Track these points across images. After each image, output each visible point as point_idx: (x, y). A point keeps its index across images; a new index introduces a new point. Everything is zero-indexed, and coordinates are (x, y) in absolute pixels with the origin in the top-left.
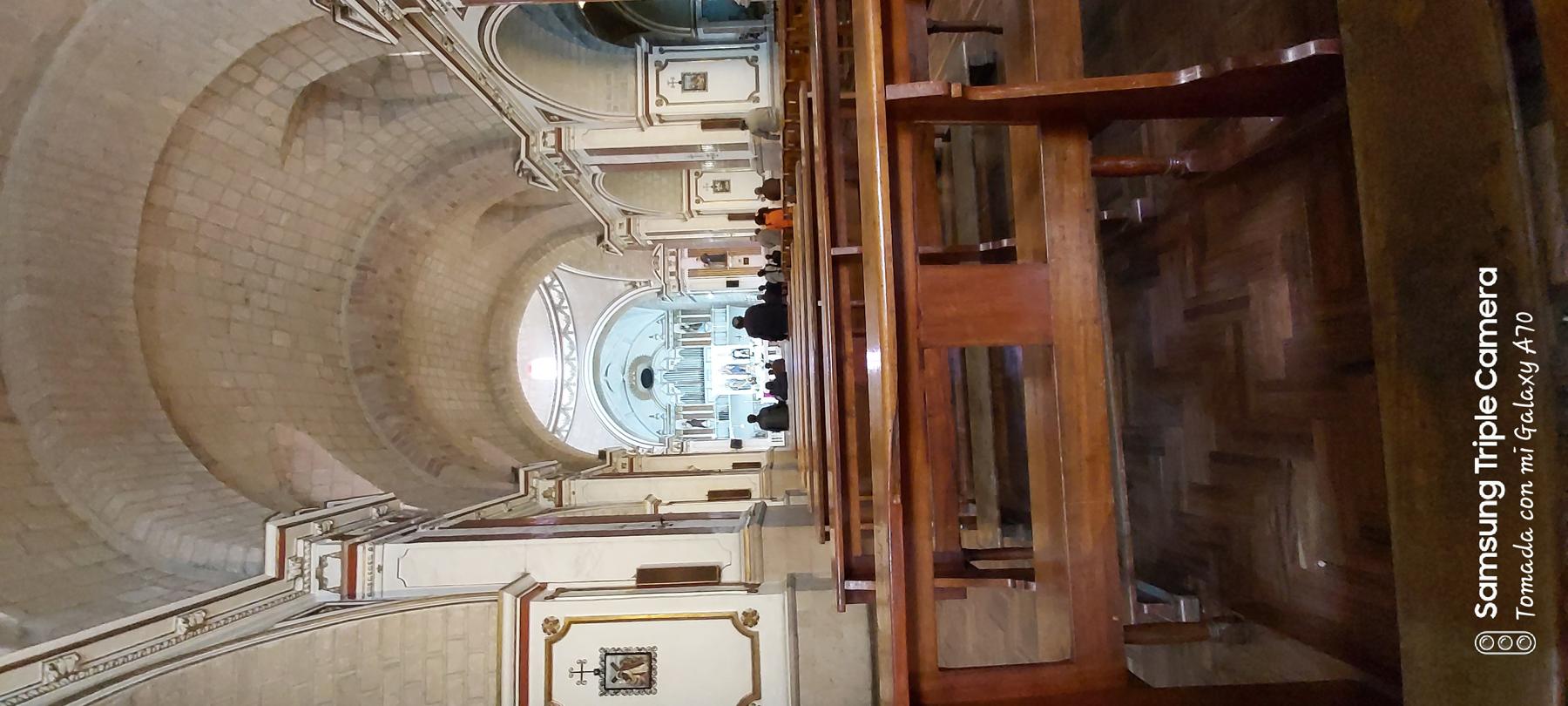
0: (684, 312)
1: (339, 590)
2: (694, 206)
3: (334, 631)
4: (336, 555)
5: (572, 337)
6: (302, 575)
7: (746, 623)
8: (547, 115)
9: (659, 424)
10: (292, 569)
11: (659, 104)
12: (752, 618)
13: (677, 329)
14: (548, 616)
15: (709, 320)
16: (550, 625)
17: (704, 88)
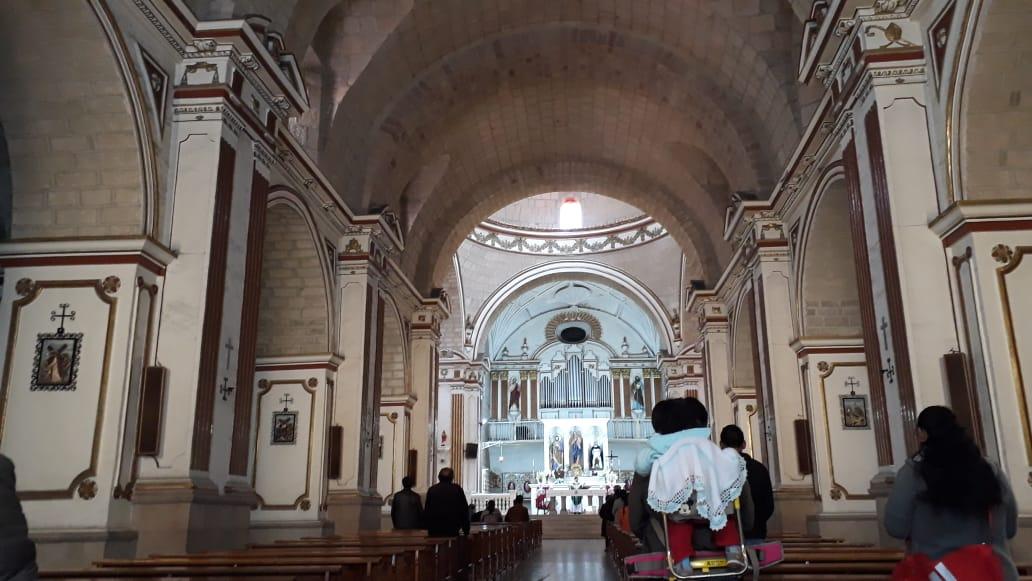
4: (216, 79)
5: (608, 247)
6: (199, 51)
7: (84, 486)
8: (795, 231)
9: (515, 350)
10: (204, 43)
11: (822, 366)
12: (88, 492)
13: (636, 372)
14: (122, 282)
16: (113, 283)
17: (847, 425)
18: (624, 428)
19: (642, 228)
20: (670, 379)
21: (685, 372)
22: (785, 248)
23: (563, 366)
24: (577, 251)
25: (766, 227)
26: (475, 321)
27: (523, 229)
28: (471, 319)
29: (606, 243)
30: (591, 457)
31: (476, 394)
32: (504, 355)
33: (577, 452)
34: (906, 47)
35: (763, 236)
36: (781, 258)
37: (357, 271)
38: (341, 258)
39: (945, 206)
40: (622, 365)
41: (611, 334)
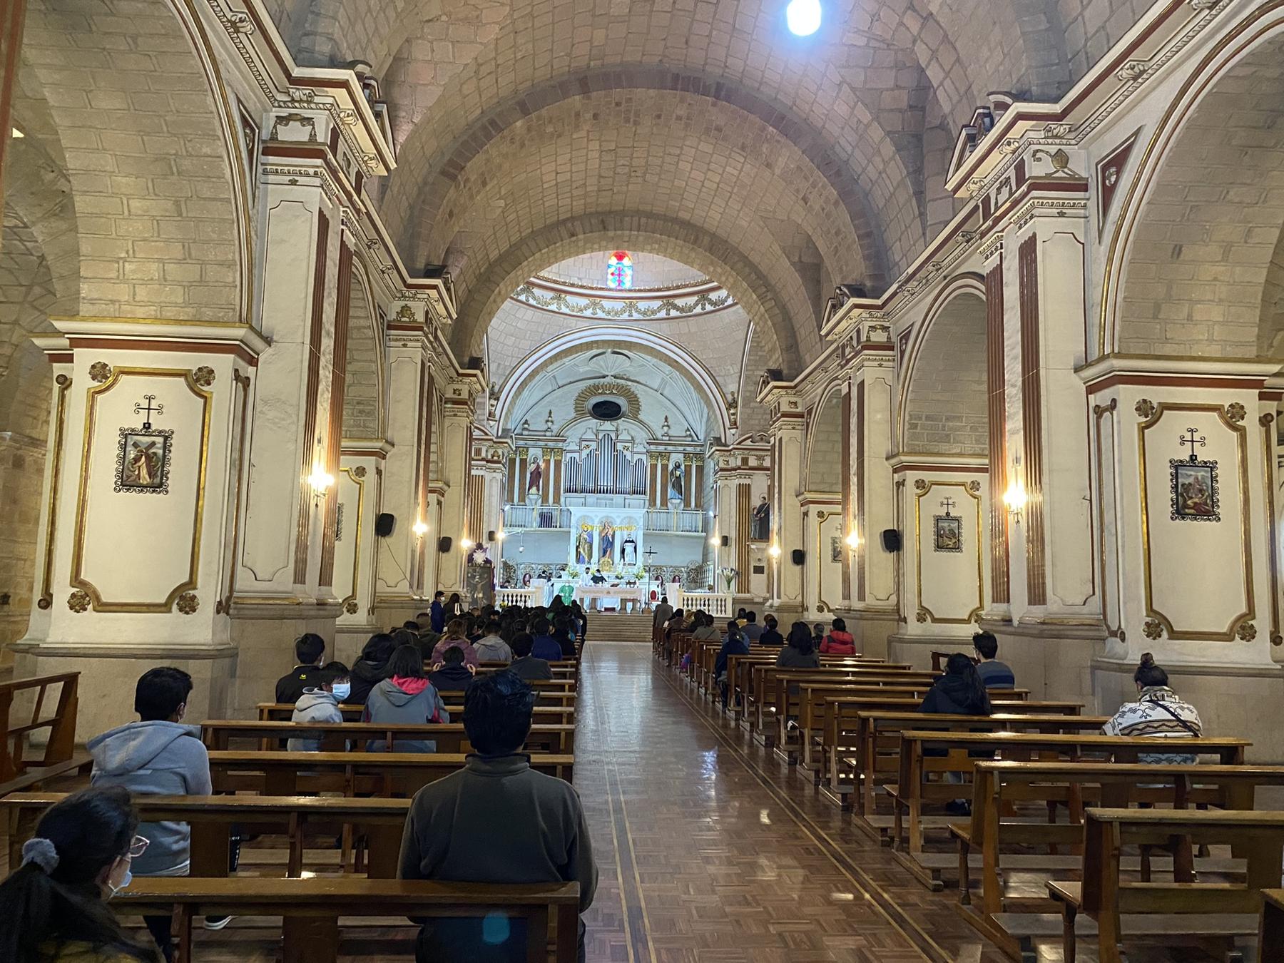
0: (700, 470)
1: (274, 137)
2: (814, 509)
3: (221, 157)
4: (313, 136)
5: (663, 314)
9: (538, 425)
10: (299, 93)
11: (920, 484)
13: (676, 457)
15: (687, 504)
17: (939, 547)
18: (660, 519)
19: (703, 295)
20: (722, 470)
21: (739, 463)
22: (891, 353)
23: (594, 445)
24: (625, 316)
25: (873, 328)
26: (500, 391)
27: (564, 284)
28: (496, 388)
29: (660, 309)
30: (623, 551)
31: (499, 476)
32: (524, 429)
33: (607, 545)
34: (1072, 177)
35: (868, 337)
36: (885, 364)
37: (410, 344)
38: (390, 327)
39: (1095, 354)
40: (661, 448)
41: (651, 413)
